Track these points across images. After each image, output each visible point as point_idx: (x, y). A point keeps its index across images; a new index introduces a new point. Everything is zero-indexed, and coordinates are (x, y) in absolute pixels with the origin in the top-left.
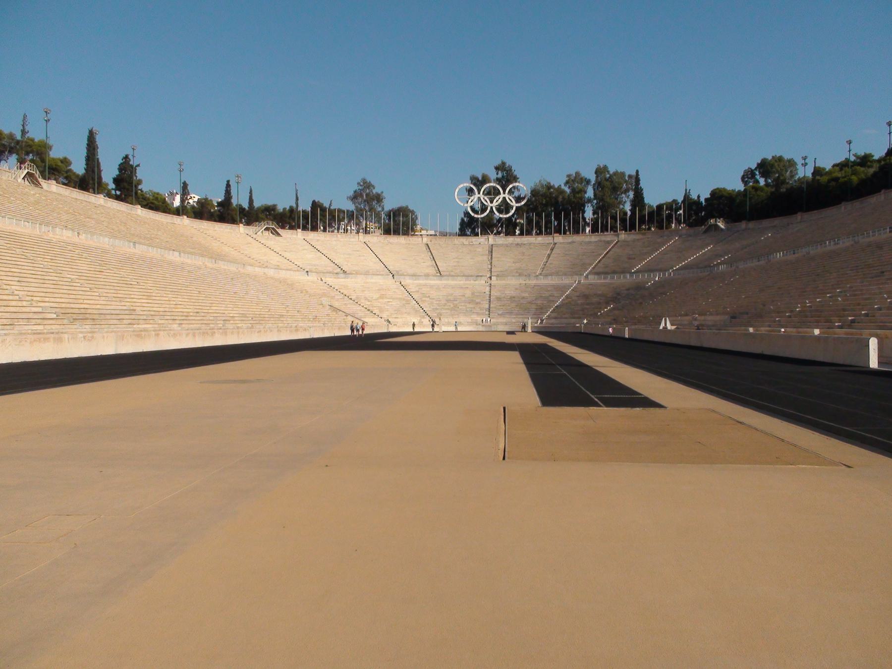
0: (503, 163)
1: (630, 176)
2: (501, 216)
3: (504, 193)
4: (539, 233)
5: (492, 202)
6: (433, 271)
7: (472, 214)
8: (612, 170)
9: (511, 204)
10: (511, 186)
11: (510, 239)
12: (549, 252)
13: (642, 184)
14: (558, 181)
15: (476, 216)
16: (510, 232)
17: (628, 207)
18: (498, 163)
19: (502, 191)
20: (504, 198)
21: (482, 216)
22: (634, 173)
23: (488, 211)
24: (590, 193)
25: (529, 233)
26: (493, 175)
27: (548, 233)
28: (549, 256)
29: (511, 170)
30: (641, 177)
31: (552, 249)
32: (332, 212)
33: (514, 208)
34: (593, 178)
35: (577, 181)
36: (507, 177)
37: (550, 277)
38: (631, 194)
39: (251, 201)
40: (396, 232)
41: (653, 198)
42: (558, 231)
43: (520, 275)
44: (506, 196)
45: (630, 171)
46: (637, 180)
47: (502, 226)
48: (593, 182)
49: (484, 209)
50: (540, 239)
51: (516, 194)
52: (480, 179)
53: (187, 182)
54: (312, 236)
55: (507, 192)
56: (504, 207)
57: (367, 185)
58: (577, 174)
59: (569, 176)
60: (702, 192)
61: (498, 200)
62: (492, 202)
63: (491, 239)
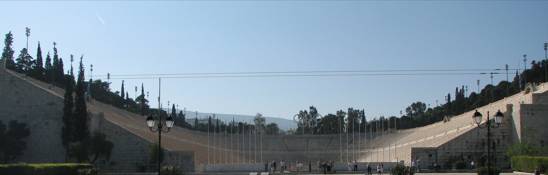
0: (313, 107)
1: (361, 111)
2: (312, 127)
3: (313, 118)
4: (327, 133)
5: (308, 121)
7: (300, 126)
8: (354, 109)
9: (316, 122)
10: (315, 115)
11: (316, 136)
12: (329, 141)
13: (365, 115)
14: (334, 113)
15: (302, 127)
16: (315, 133)
17: (361, 122)
18: (311, 106)
19: (312, 117)
20: (313, 120)
21: (304, 127)
22: (363, 111)
23: (306, 126)
24: (346, 116)
25: (323, 133)
26: (309, 111)
28: (330, 142)
29: (315, 108)
30: (364, 112)
31: (331, 140)
33: (317, 124)
34: (347, 111)
35: (341, 113)
36: (314, 112)
37: (330, 151)
40: (271, 134)
42: (333, 132)
43: (319, 150)
44: (314, 119)
45: (361, 110)
46: (363, 112)
47: (312, 130)
48: (347, 113)
49: (305, 124)
50: (327, 135)
51: (317, 118)
52: (303, 111)
53: (197, 118)
55: (314, 117)
56: (313, 123)
57: (261, 115)
58: (341, 111)
59: (338, 112)
60: (387, 116)
61: (311, 120)
62: (308, 121)
63: (308, 135)
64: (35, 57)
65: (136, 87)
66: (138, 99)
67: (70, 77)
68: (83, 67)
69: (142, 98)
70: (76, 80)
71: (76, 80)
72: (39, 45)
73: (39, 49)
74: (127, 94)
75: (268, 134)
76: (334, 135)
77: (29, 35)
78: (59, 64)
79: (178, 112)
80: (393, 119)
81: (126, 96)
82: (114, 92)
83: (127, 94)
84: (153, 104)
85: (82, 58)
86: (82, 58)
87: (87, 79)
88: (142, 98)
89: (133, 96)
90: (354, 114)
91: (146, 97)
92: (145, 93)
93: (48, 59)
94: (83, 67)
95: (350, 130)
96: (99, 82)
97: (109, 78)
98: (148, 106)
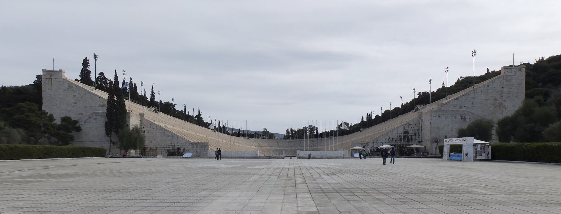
6: (278, 146)
11: (293, 140)
27: (300, 139)
32: (259, 135)
38: (316, 131)
39: (244, 132)
40: (271, 139)
41: (320, 132)
46: (317, 128)
50: (299, 140)
54: (255, 139)
58: (306, 127)
60: (329, 130)
64: (113, 80)
65: (194, 109)
66: (196, 117)
67: (145, 98)
68: (154, 92)
69: (199, 116)
70: (149, 99)
71: (149, 99)
72: (116, 72)
73: (116, 75)
74: (188, 112)
75: (269, 139)
76: (302, 140)
77: (97, 59)
78: (133, 88)
79: (222, 126)
80: (332, 131)
81: (187, 114)
82: (179, 111)
83: (188, 112)
84: (205, 120)
85: (153, 86)
86: (153, 86)
87: (157, 99)
88: (199, 116)
89: (194, 114)
90: (312, 129)
91: (201, 116)
92: (201, 113)
93: (124, 83)
94: (154, 92)
95: (311, 136)
96: (168, 103)
97: (173, 101)
98: (203, 121)
